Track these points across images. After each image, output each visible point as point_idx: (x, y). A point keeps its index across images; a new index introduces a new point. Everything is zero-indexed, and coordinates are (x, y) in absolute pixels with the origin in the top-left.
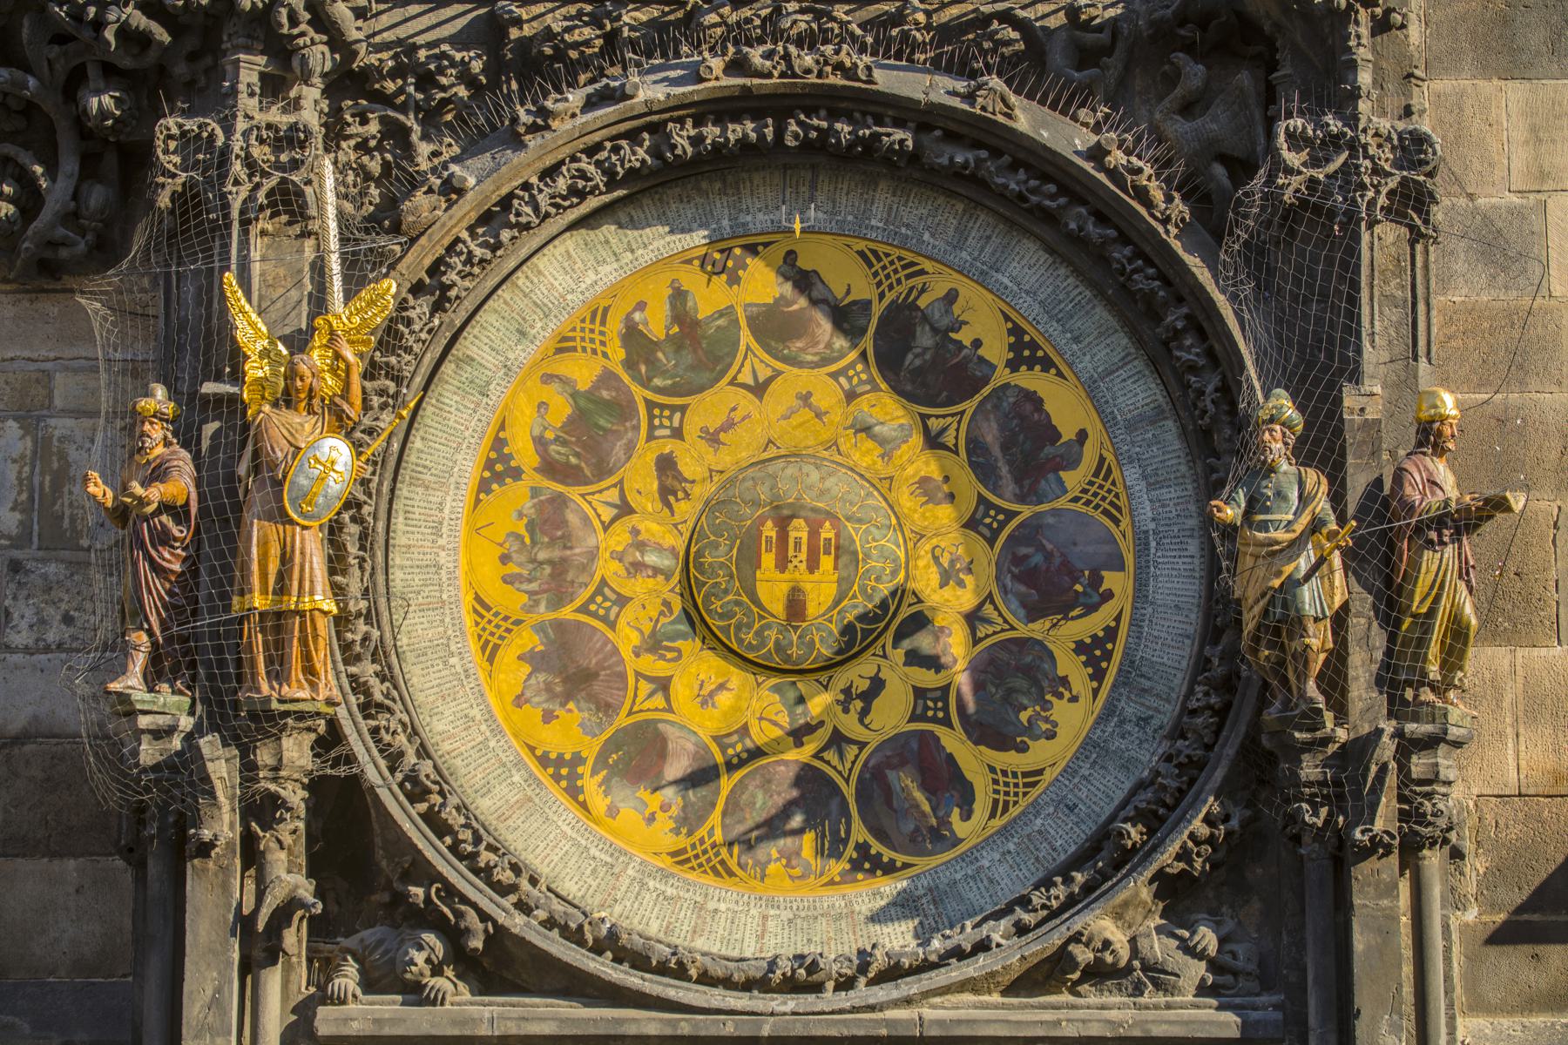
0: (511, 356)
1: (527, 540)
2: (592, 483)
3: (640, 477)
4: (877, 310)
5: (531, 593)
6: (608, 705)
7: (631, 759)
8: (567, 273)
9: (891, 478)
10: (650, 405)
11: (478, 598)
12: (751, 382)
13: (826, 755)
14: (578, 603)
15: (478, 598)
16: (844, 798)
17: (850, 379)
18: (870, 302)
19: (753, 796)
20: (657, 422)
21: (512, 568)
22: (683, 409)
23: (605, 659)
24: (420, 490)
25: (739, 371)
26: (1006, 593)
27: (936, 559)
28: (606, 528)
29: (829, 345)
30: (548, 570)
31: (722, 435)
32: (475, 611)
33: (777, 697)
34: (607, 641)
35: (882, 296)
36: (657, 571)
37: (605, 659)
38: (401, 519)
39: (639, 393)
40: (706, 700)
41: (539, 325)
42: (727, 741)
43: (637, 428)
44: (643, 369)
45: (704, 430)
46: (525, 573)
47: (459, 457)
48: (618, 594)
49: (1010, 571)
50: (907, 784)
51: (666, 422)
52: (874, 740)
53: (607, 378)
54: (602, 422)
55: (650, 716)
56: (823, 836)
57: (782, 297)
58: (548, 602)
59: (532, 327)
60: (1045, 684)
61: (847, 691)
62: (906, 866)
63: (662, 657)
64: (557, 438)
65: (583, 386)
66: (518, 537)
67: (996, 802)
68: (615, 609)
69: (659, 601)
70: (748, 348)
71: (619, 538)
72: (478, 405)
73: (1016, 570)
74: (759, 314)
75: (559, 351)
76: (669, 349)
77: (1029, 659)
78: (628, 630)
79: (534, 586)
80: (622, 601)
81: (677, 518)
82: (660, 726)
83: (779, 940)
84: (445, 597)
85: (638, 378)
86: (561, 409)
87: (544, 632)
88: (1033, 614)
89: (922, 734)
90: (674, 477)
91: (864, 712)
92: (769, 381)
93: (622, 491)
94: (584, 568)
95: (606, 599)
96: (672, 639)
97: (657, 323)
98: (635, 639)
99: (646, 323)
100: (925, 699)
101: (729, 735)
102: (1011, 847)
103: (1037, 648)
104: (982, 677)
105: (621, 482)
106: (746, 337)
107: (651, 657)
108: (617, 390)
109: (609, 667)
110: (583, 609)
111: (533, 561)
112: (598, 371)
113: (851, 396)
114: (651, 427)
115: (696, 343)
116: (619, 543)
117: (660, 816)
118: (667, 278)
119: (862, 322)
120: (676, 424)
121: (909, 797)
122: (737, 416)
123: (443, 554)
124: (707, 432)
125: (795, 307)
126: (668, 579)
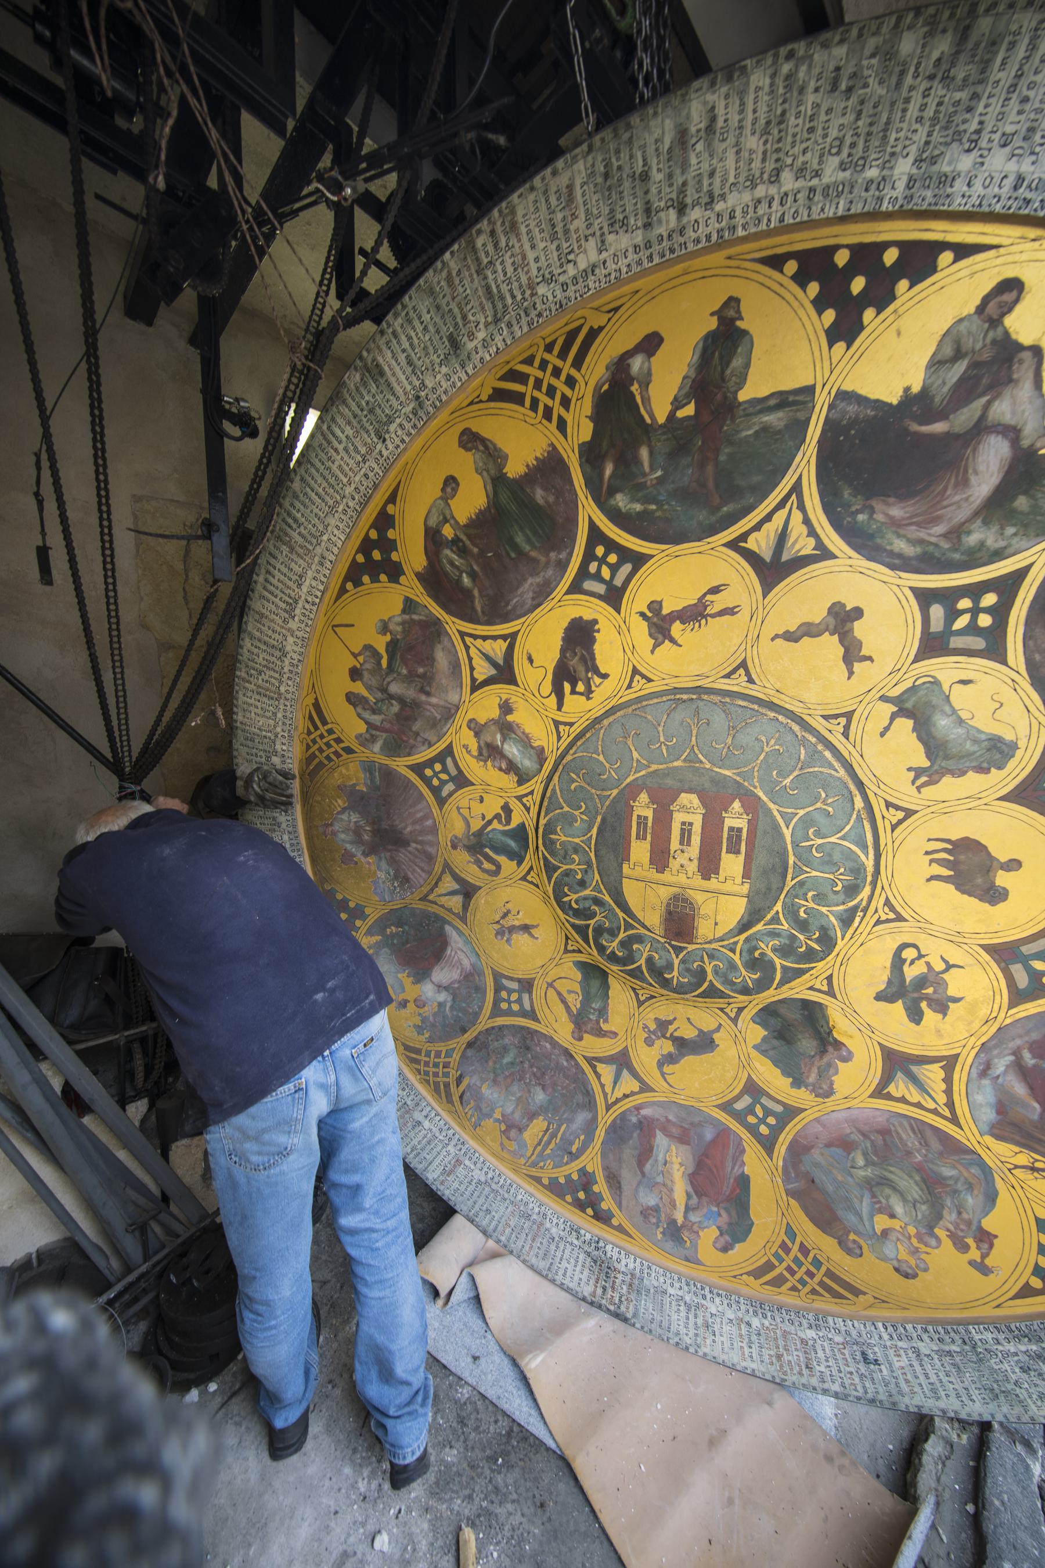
0: (430, 383)
1: (384, 663)
2: (478, 623)
3: (541, 636)
6: (406, 879)
7: (407, 942)
8: (554, 237)
9: (909, 813)
10: (596, 535)
11: (316, 705)
12: (767, 556)
13: (601, 1067)
15: (316, 705)
16: (595, 1119)
19: (505, 1049)
20: (593, 567)
21: (359, 688)
23: (421, 832)
24: (285, 549)
25: (757, 527)
26: (984, 1073)
27: (898, 962)
28: (475, 687)
29: (956, 533)
30: (396, 708)
31: (676, 628)
32: (311, 718)
33: (579, 976)
34: (429, 815)
36: (511, 767)
37: (421, 832)
38: (261, 579)
39: (588, 510)
40: (505, 932)
41: (481, 335)
42: (505, 982)
43: (562, 566)
44: (609, 470)
45: (655, 606)
47: (332, 521)
48: (460, 771)
49: (1017, 1053)
50: (674, 1162)
51: (606, 573)
52: (662, 1093)
53: (551, 466)
54: (520, 539)
55: (441, 912)
56: (554, 1135)
59: (471, 336)
60: (950, 1217)
61: (663, 1025)
62: (620, 1229)
63: (479, 863)
64: (456, 540)
65: (514, 469)
67: (768, 1267)
68: (450, 787)
69: (502, 802)
71: (485, 706)
72: (371, 450)
73: (1029, 1059)
74: (854, 422)
75: (499, 395)
76: (662, 446)
77: (947, 1172)
78: (454, 814)
79: (376, 719)
80: (462, 781)
82: (447, 928)
83: (462, 1188)
84: (283, 689)
85: (593, 485)
86: (471, 500)
87: (371, 774)
88: (1008, 1126)
89: (723, 1134)
90: (583, 659)
91: (670, 1059)
92: (801, 562)
95: (445, 770)
96: (497, 850)
99: (646, 382)
100: (756, 1101)
101: (511, 979)
102: (756, 1322)
103: (975, 1170)
104: (856, 1137)
105: (514, 636)
106: (805, 465)
109: (422, 843)
110: (418, 769)
111: (384, 690)
113: (933, 645)
114: (583, 573)
117: (411, 1006)
120: (618, 582)
121: (666, 1174)
122: (719, 602)
123: (291, 640)
125: (939, 427)
126: (521, 782)
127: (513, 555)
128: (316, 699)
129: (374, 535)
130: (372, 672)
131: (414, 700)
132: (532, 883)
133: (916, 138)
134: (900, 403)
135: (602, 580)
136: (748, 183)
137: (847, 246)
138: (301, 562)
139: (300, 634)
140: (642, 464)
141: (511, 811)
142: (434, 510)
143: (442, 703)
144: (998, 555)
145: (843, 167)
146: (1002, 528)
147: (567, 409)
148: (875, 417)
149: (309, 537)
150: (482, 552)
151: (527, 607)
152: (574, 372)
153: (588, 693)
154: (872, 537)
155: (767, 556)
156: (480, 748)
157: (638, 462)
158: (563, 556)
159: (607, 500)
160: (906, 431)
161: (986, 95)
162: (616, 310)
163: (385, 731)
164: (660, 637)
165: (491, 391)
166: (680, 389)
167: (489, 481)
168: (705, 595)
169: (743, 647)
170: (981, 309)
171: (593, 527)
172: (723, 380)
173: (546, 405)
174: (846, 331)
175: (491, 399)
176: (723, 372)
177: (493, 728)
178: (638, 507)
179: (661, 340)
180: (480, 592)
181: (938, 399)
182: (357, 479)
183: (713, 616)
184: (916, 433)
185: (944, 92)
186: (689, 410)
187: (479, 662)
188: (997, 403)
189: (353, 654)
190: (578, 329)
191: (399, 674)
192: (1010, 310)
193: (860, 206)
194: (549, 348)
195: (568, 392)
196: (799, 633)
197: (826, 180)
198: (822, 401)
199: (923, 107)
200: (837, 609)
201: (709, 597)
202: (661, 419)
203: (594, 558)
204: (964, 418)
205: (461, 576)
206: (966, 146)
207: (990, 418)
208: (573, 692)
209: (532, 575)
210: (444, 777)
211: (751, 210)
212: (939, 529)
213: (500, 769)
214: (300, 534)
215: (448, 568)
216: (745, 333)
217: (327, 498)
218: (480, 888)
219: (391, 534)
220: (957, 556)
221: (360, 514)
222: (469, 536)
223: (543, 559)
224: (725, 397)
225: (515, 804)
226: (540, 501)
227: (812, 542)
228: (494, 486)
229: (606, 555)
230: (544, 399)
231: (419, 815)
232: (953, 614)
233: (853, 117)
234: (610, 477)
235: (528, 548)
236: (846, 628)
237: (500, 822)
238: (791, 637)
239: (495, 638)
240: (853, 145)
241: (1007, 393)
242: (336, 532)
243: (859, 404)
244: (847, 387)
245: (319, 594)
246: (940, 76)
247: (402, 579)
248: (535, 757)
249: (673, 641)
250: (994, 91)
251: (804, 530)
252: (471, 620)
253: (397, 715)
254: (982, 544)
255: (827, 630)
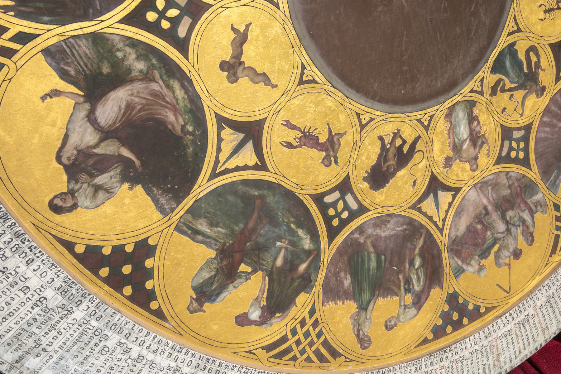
1: (496, 247)
2: (428, 232)
3: (400, 193)
4: (51, 34)
5: (532, 213)
10: (333, 233)
12: (250, 146)
14: (522, 170)
17: (175, 22)
18: (46, 52)
21: (521, 243)
22: (318, 199)
25: (246, 168)
31: (323, 138)
34: (542, 124)
35: (23, 38)
36: (472, 119)
39: (328, 252)
43: (361, 229)
44: (303, 267)
45: (326, 162)
46: (520, 230)
47: (466, 353)
48: (503, 141)
51: (340, 205)
54: (373, 264)
57: (124, 178)
58: (532, 195)
64: (408, 290)
66: (497, 257)
68: (517, 135)
69: (494, 99)
70: (214, 175)
71: (460, 174)
74: (166, 191)
75: (335, 354)
76: (268, 258)
78: (527, 113)
79: (526, 216)
80: (507, 133)
81: (421, 131)
87: (555, 181)
90: (386, 160)
92: (236, 126)
93: (421, 200)
94: (495, 185)
95: (511, 149)
97: (249, 291)
98: (532, 99)
106: (203, 186)
107: (541, 75)
108: (336, 274)
111: (508, 230)
112: (331, 306)
114: (353, 215)
115: (243, 237)
116: (463, 170)
118: (194, 321)
119: (85, 47)
122: (292, 136)
124: (327, 157)
125: (126, 153)
127: (383, 257)
128: (551, 256)
129: (449, 329)
130: (507, 247)
131: (496, 211)
132: (516, 23)
133: (65, 325)
134: (138, 183)
135: (345, 202)
136: (154, 365)
137: (122, 295)
138: (499, 344)
139: (531, 302)
140: (284, 256)
141: (492, 88)
142: (408, 317)
143: (481, 195)
144: (133, 43)
145: (107, 337)
146: (123, 60)
147: (304, 319)
148: (154, 186)
149: (485, 354)
150: (399, 272)
151: (395, 219)
152: (290, 336)
153: (397, 135)
154: (191, 111)
155: (250, 146)
156: (481, 147)
157: (285, 259)
158: (356, 235)
159: (314, 250)
160: (143, 164)
161: (24, 321)
162: (250, 352)
163: (526, 204)
164: (335, 140)
165: (337, 359)
166: (241, 283)
167: (369, 310)
168: (296, 147)
169: (294, 95)
170: (75, 206)
171: (331, 238)
172: (217, 271)
173: (314, 329)
174: (145, 249)
175: (340, 355)
176: (215, 275)
177: (464, 155)
178: (300, 232)
179: (236, 318)
180: (414, 250)
181: (118, 170)
182: (437, 366)
183: (299, 129)
184: (138, 158)
185: (42, 338)
186: (243, 267)
187: (444, 206)
188: (91, 143)
189: (509, 268)
190: (274, 357)
191: (493, 234)
192: (61, 194)
193: (108, 311)
194: (294, 359)
195: (298, 327)
196: (260, 78)
197: (118, 337)
198: (176, 217)
199: (55, 338)
200: (233, 78)
201: (295, 144)
202: (260, 273)
203: (341, 220)
204: (110, 148)
205: (419, 268)
206: (45, 301)
207: (98, 137)
208: (404, 142)
209: (381, 237)
210: (514, 144)
211: (160, 351)
212: (155, 87)
213: (479, 123)
214: (488, 360)
215: (422, 278)
216: (194, 289)
217: (460, 368)
218: (550, 45)
219: (440, 322)
220: (154, 61)
221: (449, 346)
222: (399, 288)
223: (369, 242)
224: (222, 260)
225: (487, 91)
226: (349, 277)
227: (224, 134)
228: (367, 306)
229: (334, 217)
230: (313, 334)
231: (547, 129)
232: (175, 22)
233: (89, 359)
234: (305, 262)
235: (373, 256)
236: (234, 60)
237: (504, 85)
238: (265, 79)
239: (425, 214)
240: (96, 345)
241: (83, 146)
242: (469, 346)
243: (158, 200)
244: (158, 215)
245: (503, 318)
246: (40, 348)
247: (451, 292)
248: (454, 115)
249: (330, 132)
250: (20, 320)
251: (223, 145)
252: (429, 235)
253: (512, 209)
254: (138, 58)
255: (245, 68)
